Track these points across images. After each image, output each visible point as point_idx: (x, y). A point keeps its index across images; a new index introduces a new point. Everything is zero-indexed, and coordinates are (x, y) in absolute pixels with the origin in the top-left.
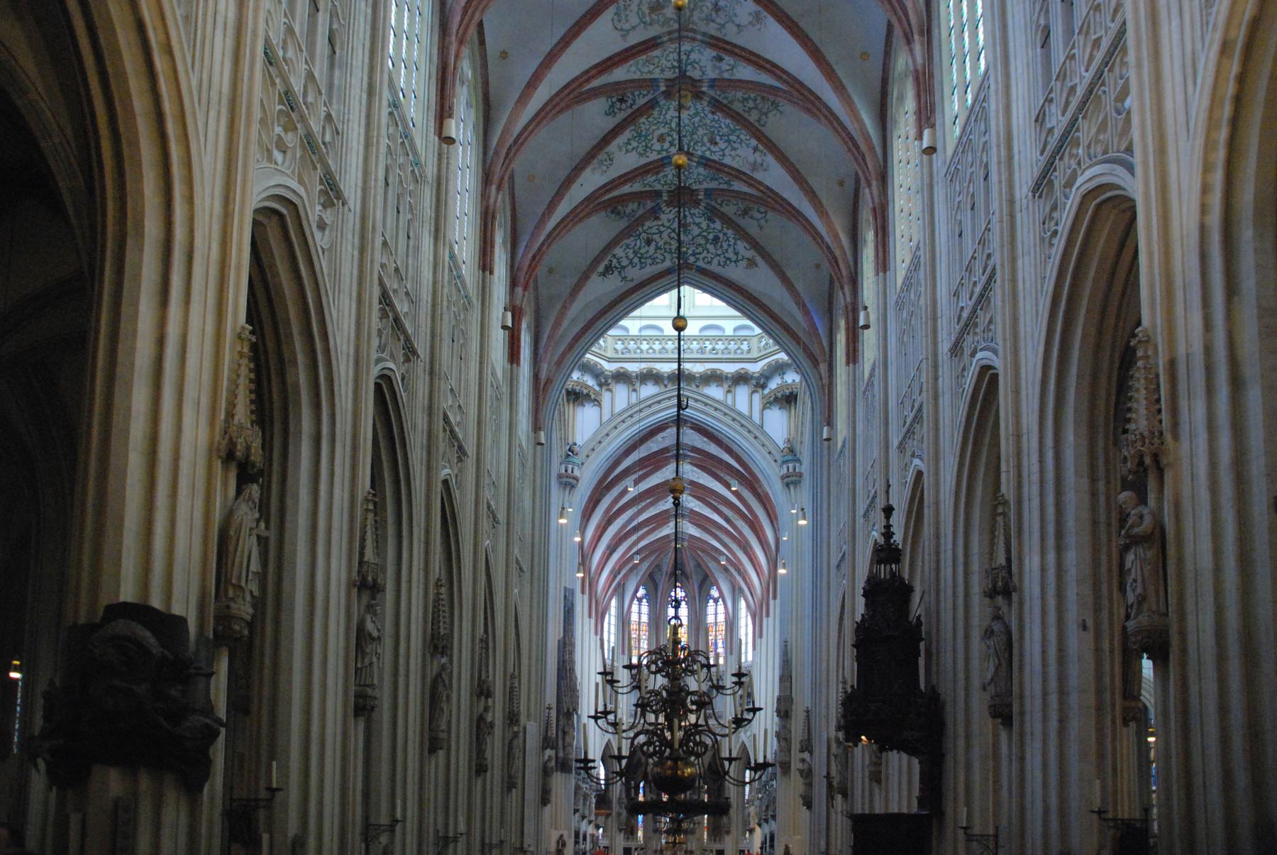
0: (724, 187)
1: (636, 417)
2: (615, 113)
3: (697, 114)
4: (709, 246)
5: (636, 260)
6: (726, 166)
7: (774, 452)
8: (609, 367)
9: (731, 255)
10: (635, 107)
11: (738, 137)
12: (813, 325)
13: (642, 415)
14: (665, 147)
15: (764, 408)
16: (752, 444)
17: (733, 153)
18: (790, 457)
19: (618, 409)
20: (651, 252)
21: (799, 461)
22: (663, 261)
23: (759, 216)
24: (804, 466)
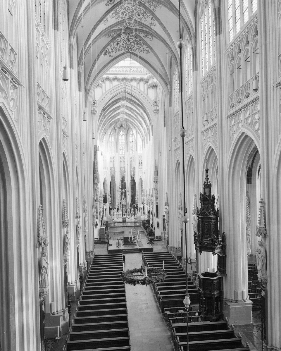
2: (109, 5)
3: (134, 6)
4: (135, 46)
5: (114, 50)
6: (142, 23)
9: (142, 49)
10: (115, 3)
11: (147, 14)
14: (124, 16)
15: (148, 89)
17: (145, 19)
18: (156, 104)
19: (107, 89)
20: (118, 47)
22: (122, 50)
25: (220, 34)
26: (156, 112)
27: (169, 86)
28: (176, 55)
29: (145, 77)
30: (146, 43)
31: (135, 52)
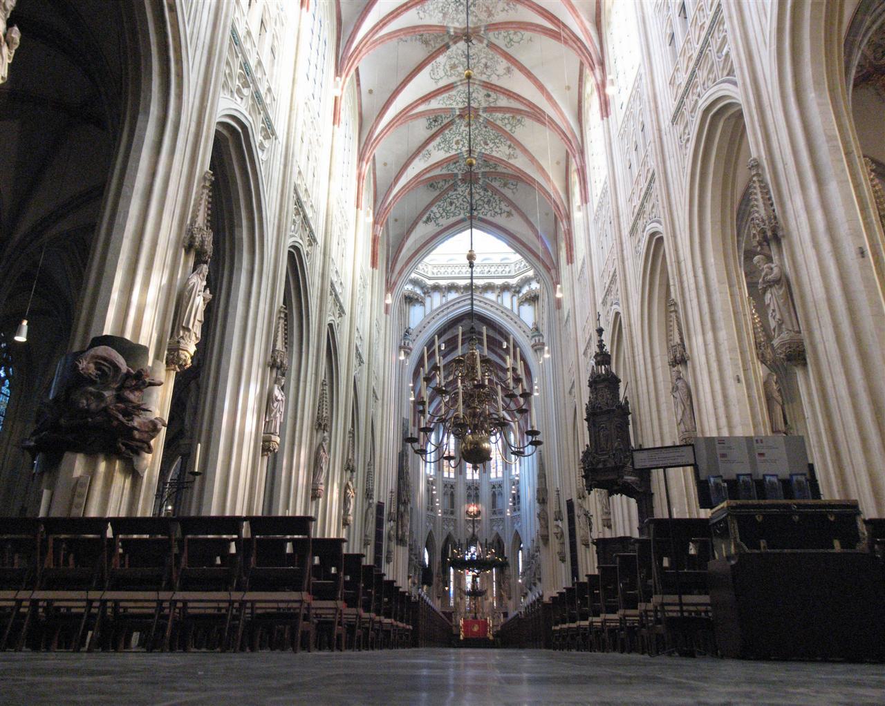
0: (493, 170)
1: (445, 312)
5: (444, 214)
6: (493, 157)
7: (527, 331)
8: (430, 283)
9: (497, 210)
12: (546, 248)
13: (449, 310)
16: (513, 326)
18: (536, 333)
19: (435, 307)
20: (453, 210)
21: (541, 335)
22: (459, 214)
23: (512, 187)
24: (545, 339)
25: (607, 117)
26: (539, 349)
27: (553, 272)
28: (558, 202)
29: (513, 282)
30: (504, 198)
31: (485, 217)
